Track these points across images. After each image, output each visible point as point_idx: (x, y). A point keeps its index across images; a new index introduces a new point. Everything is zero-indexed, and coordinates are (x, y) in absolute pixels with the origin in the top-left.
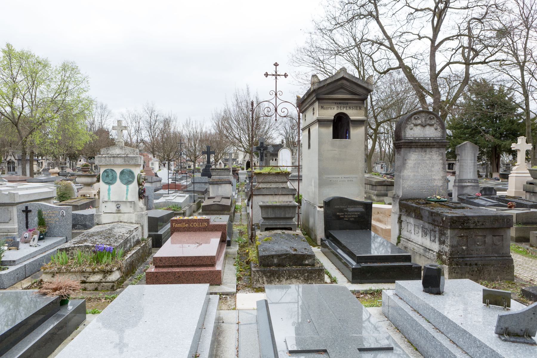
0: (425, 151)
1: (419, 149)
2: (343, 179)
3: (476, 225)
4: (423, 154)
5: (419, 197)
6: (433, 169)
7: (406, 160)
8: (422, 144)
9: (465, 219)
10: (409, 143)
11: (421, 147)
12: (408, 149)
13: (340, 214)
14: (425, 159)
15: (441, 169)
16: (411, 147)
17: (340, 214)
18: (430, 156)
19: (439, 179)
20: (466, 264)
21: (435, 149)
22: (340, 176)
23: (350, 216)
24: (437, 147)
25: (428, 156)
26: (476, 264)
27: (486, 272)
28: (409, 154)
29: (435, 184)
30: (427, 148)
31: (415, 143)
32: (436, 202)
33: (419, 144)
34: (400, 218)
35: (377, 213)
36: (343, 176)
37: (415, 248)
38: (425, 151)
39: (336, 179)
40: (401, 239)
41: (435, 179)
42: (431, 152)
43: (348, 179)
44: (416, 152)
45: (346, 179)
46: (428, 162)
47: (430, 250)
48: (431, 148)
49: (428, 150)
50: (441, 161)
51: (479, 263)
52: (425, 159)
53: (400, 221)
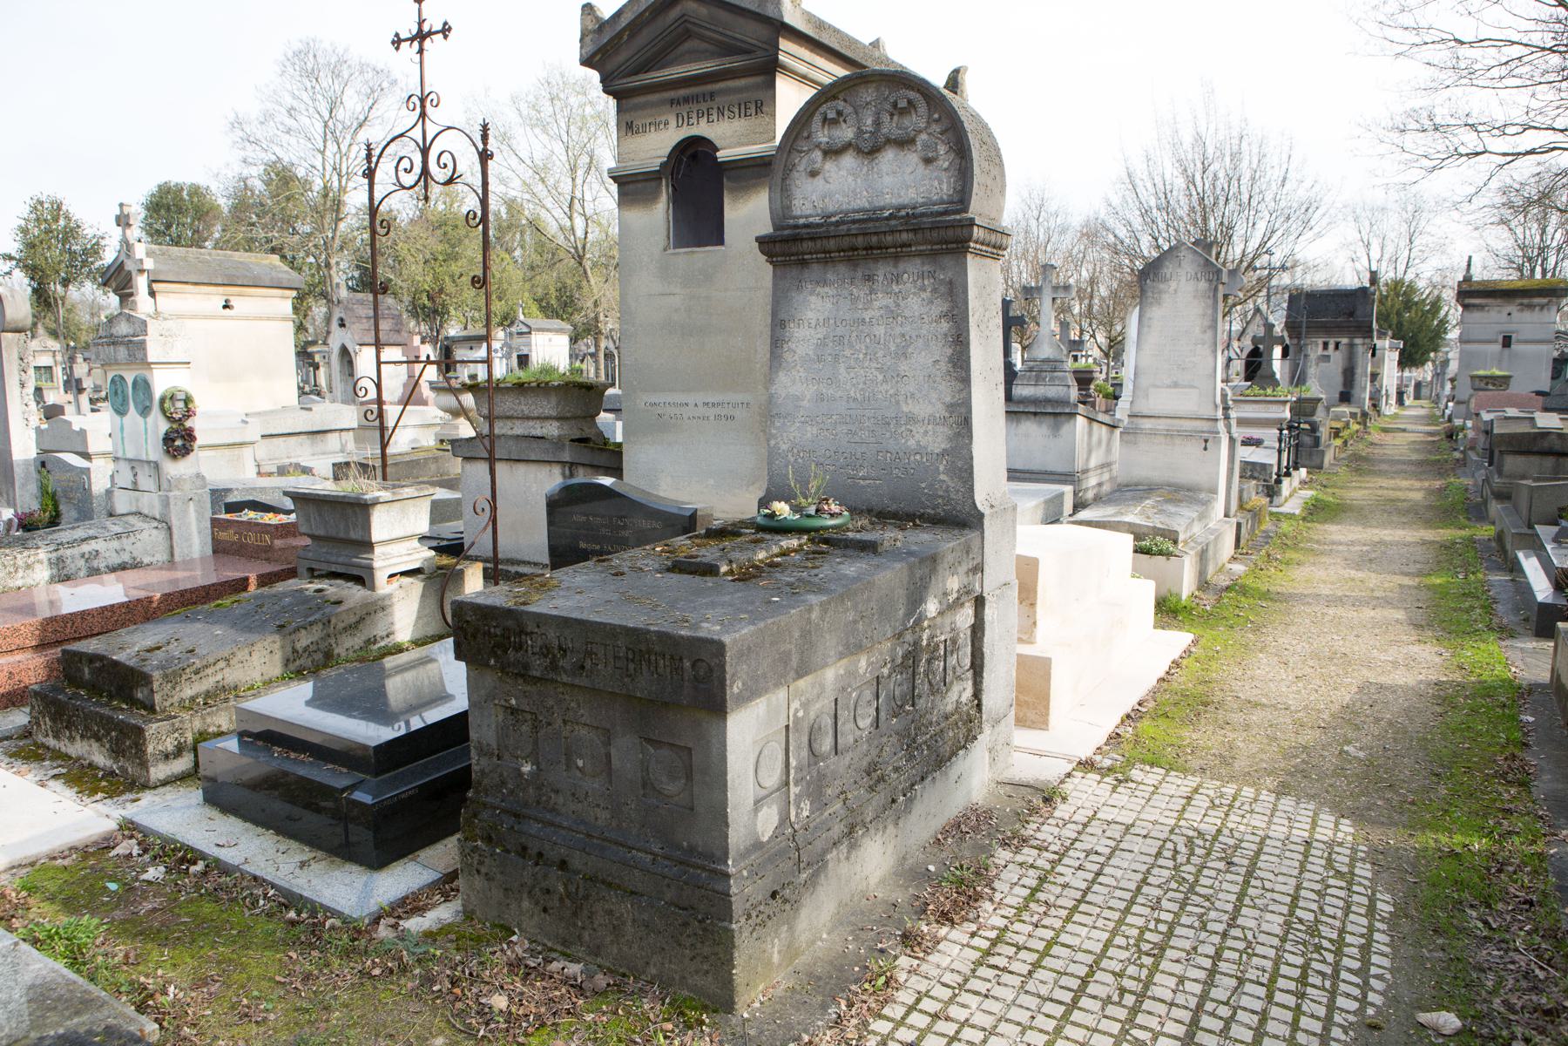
0: (869, 278)
1: (842, 269)
2: (702, 411)
3: (554, 666)
4: (860, 291)
6: (903, 367)
8: (846, 242)
9: (510, 623)
11: (849, 259)
12: (794, 272)
14: (867, 315)
15: (944, 366)
16: (803, 263)
18: (889, 301)
19: (932, 420)
20: (523, 851)
21: (912, 267)
22: (691, 398)
24: (920, 254)
25: (882, 300)
26: (563, 865)
27: (600, 919)
28: (798, 298)
30: (876, 260)
33: (832, 242)
36: (700, 398)
38: (869, 278)
39: (677, 411)
41: (912, 419)
42: (897, 279)
43: (717, 411)
44: (825, 283)
45: (712, 412)
46: (880, 331)
48: (897, 258)
49: (882, 270)
50: (945, 326)
51: (576, 861)
52: (867, 315)
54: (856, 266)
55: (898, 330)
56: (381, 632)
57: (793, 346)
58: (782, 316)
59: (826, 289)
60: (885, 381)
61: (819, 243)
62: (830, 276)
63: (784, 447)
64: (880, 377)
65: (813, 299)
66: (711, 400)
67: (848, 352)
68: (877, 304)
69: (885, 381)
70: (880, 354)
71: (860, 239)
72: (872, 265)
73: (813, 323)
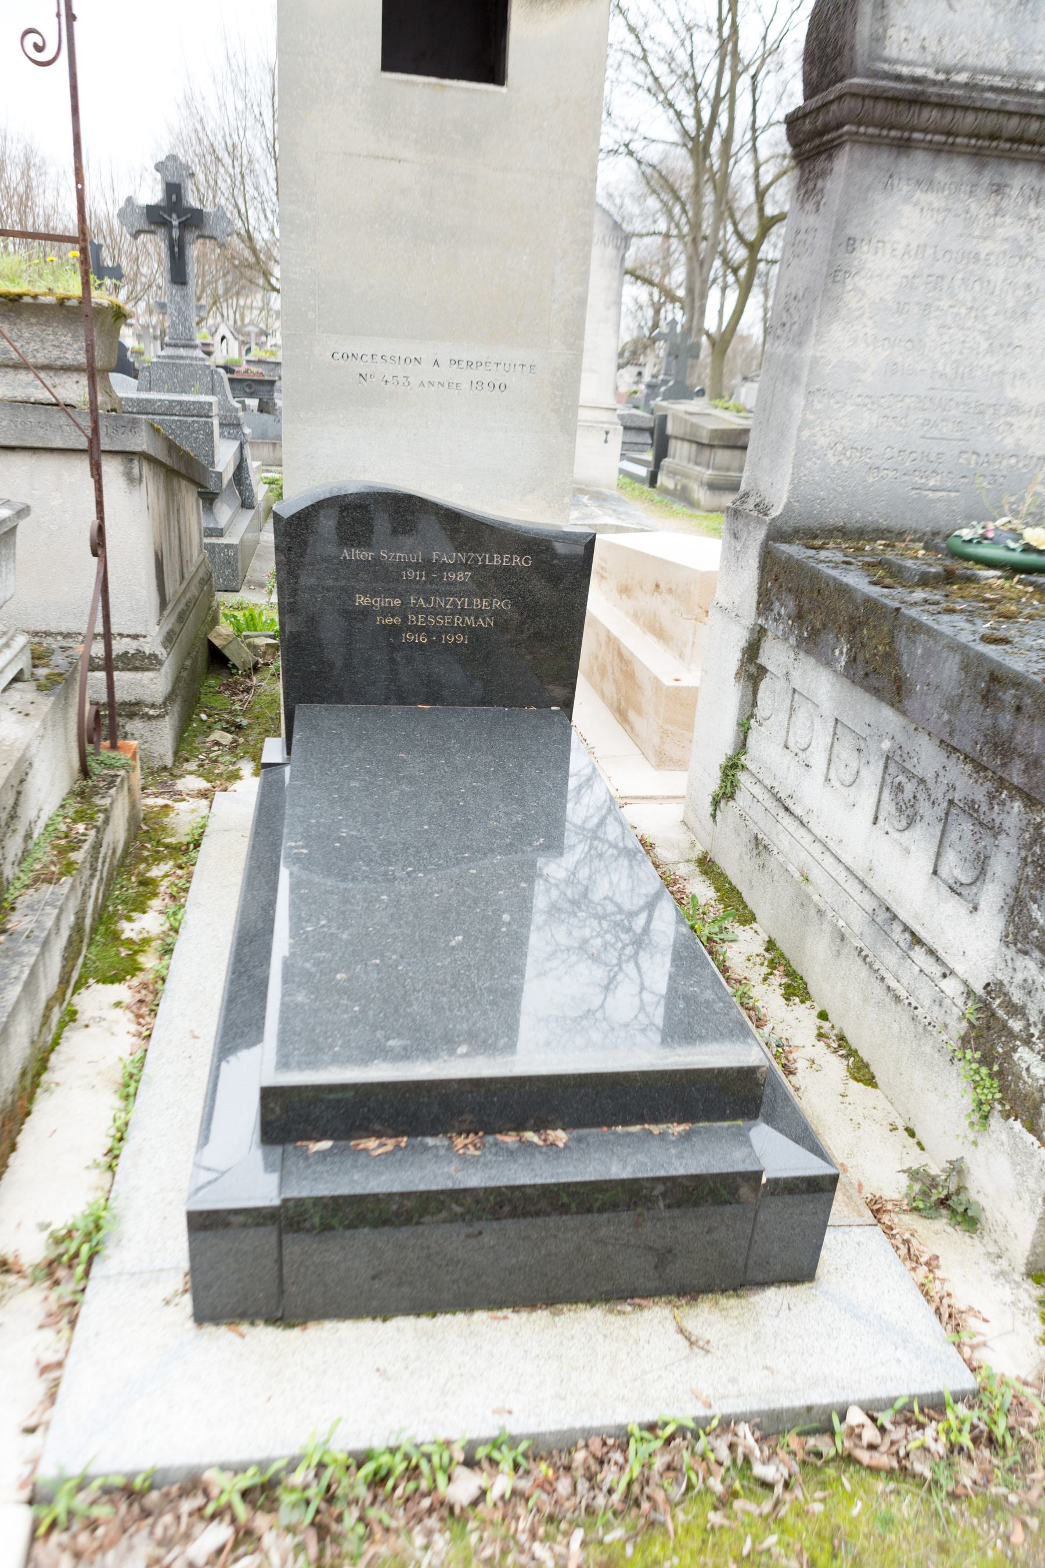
0: (998, 189)
1: (962, 167)
4: (980, 207)
5: (896, 524)
7: (851, 244)
8: (991, 122)
10: (896, 100)
12: (884, 158)
13: (379, 602)
16: (904, 146)
17: (379, 602)
23: (444, 621)
25: (1009, 228)
29: (1009, 442)
30: (1014, 159)
31: (942, 106)
32: (1013, 569)
33: (969, 120)
34: (752, 650)
35: (650, 586)
37: (816, 874)
38: (998, 189)
40: (742, 777)
41: (1016, 409)
43: (477, 374)
44: (929, 185)
46: (997, 275)
47: (917, 940)
53: (752, 671)
54: (983, 166)
55: (1024, 278)
56: (32, 814)
57: (862, 284)
58: (851, 231)
59: (931, 197)
60: (990, 350)
61: (949, 114)
62: (941, 176)
63: (823, 441)
64: (984, 345)
65: (907, 209)
66: (465, 357)
67: (945, 303)
68: (1001, 232)
69: (990, 350)
70: (991, 311)
71: (1014, 121)
72: (1006, 168)
73: (900, 248)
